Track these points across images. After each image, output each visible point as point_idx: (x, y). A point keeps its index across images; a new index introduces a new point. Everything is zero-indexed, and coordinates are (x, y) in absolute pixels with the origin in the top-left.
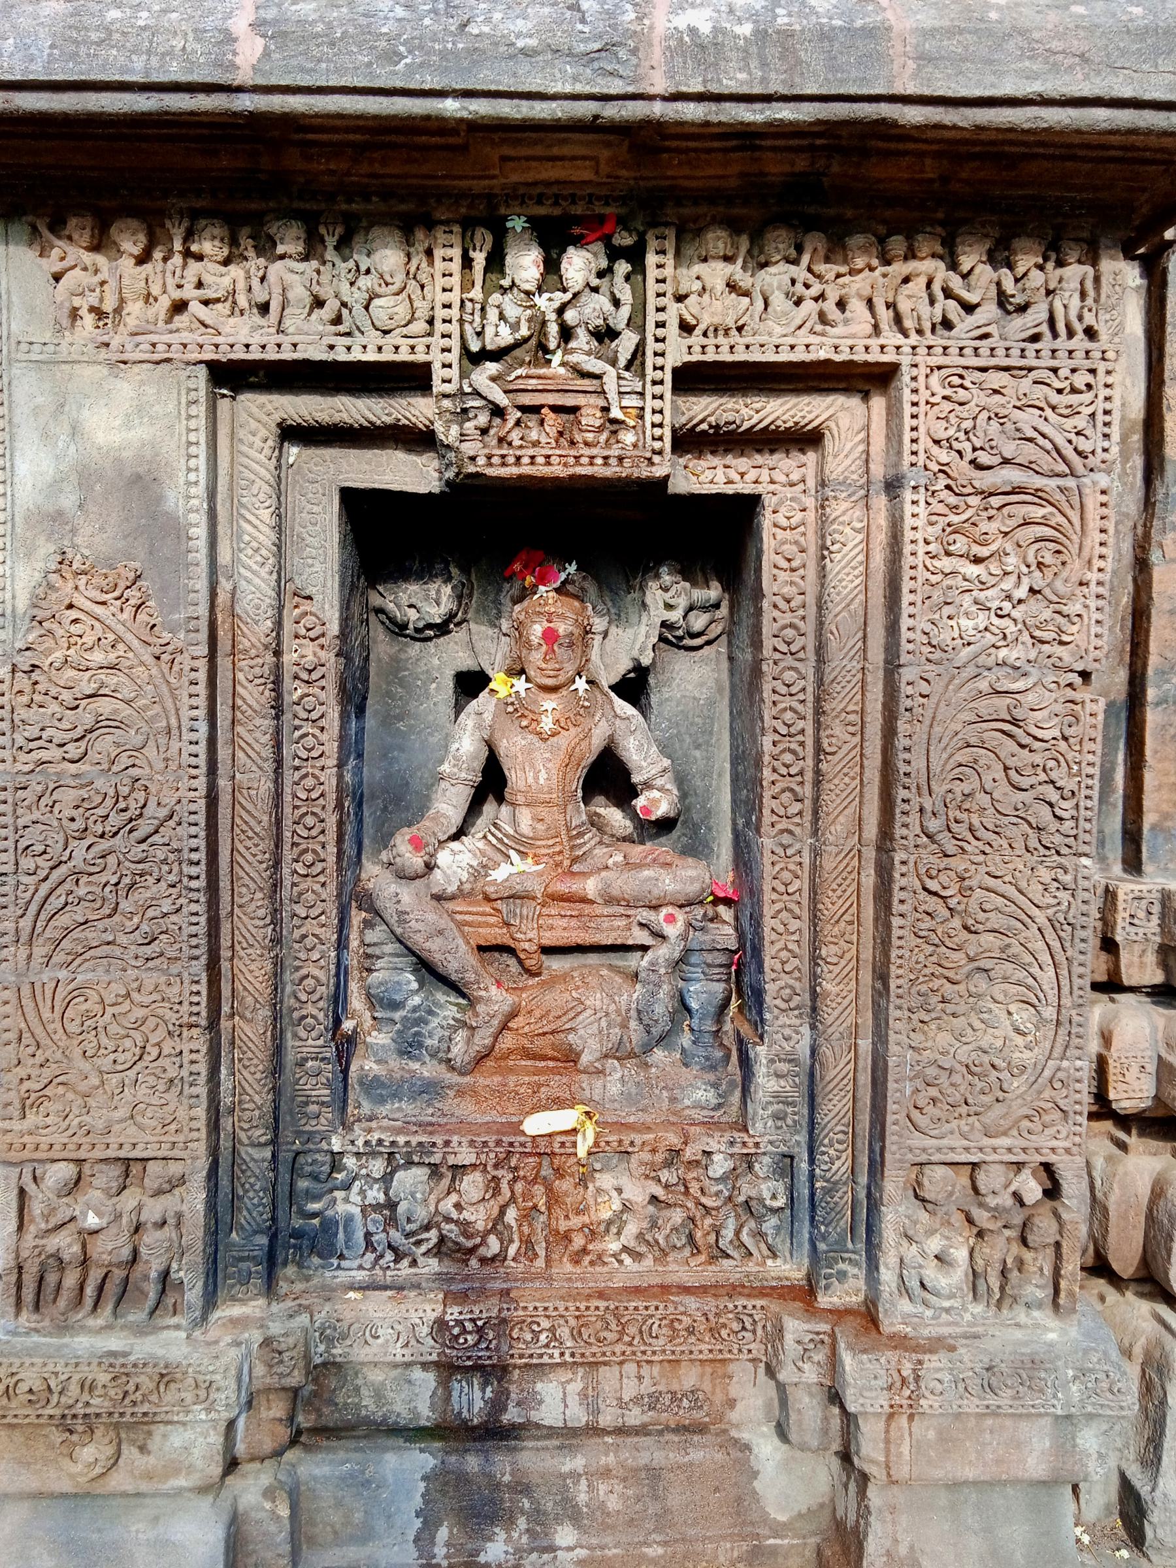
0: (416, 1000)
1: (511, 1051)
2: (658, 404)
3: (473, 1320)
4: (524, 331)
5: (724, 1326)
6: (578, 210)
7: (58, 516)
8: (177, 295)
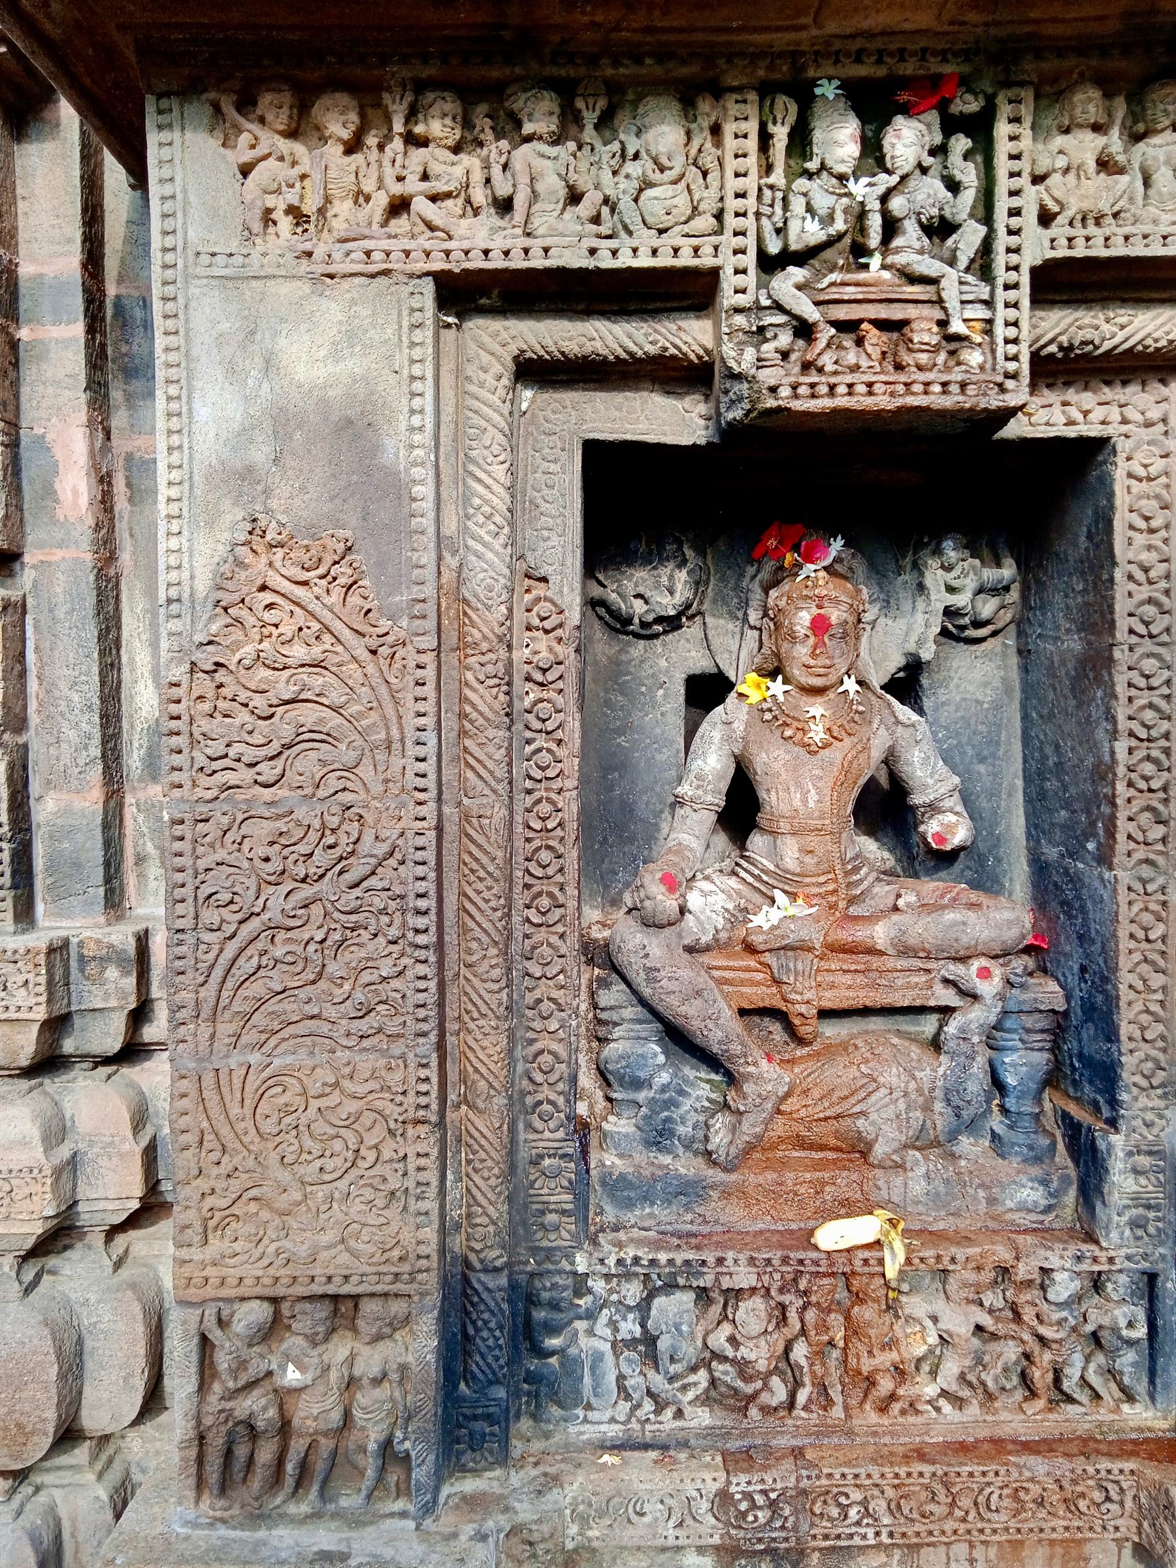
0: (664, 1077)
1: (781, 1140)
2: (1012, 314)
3: (764, 1492)
4: (840, 225)
5: (1083, 1495)
6: (909, 68)
7: (248, 474)
8: (397, 189)
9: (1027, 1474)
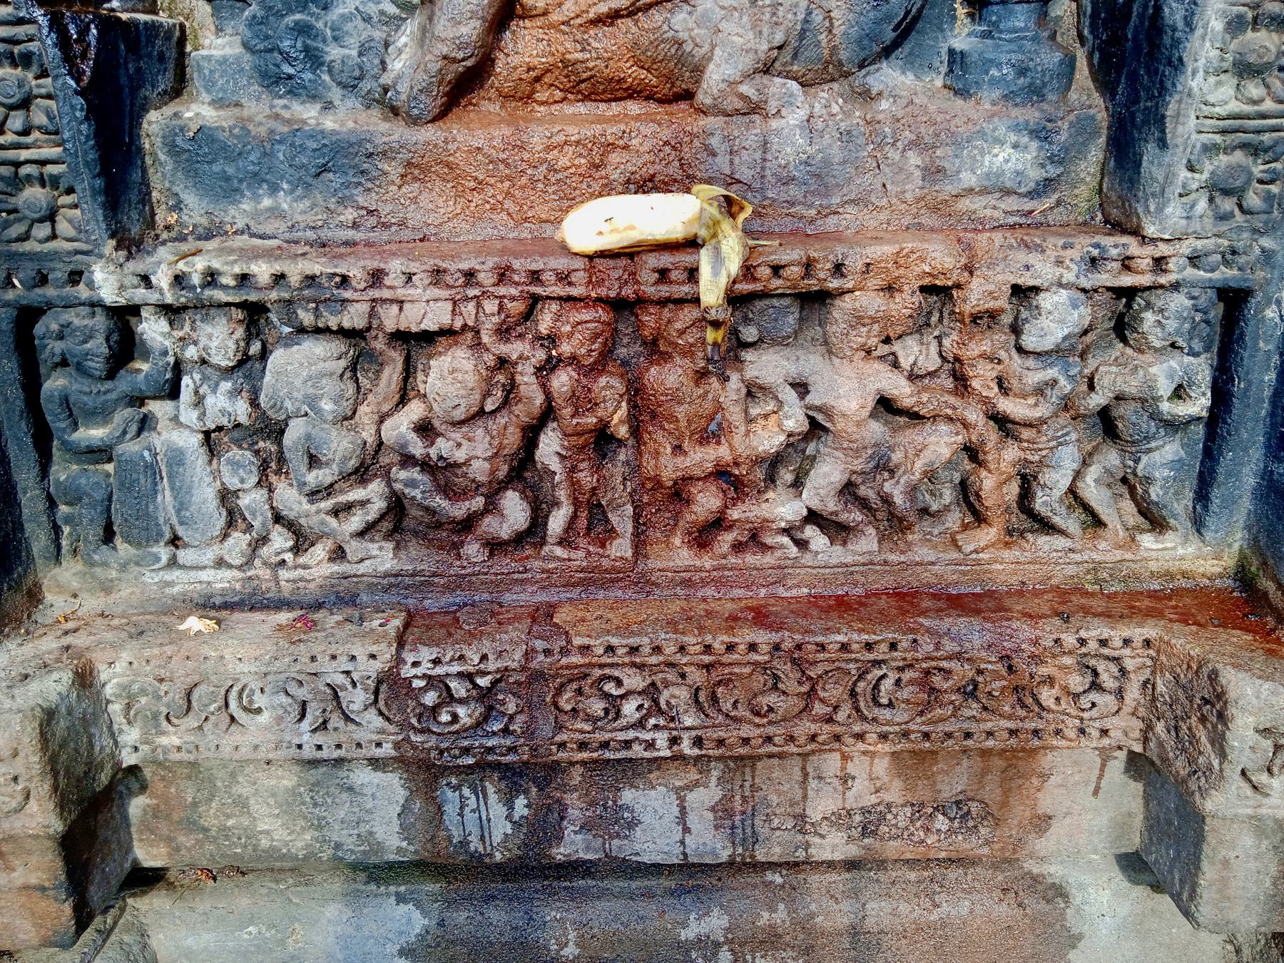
3: (469, 677)
5: (1050, 681)
9: (949, 646)
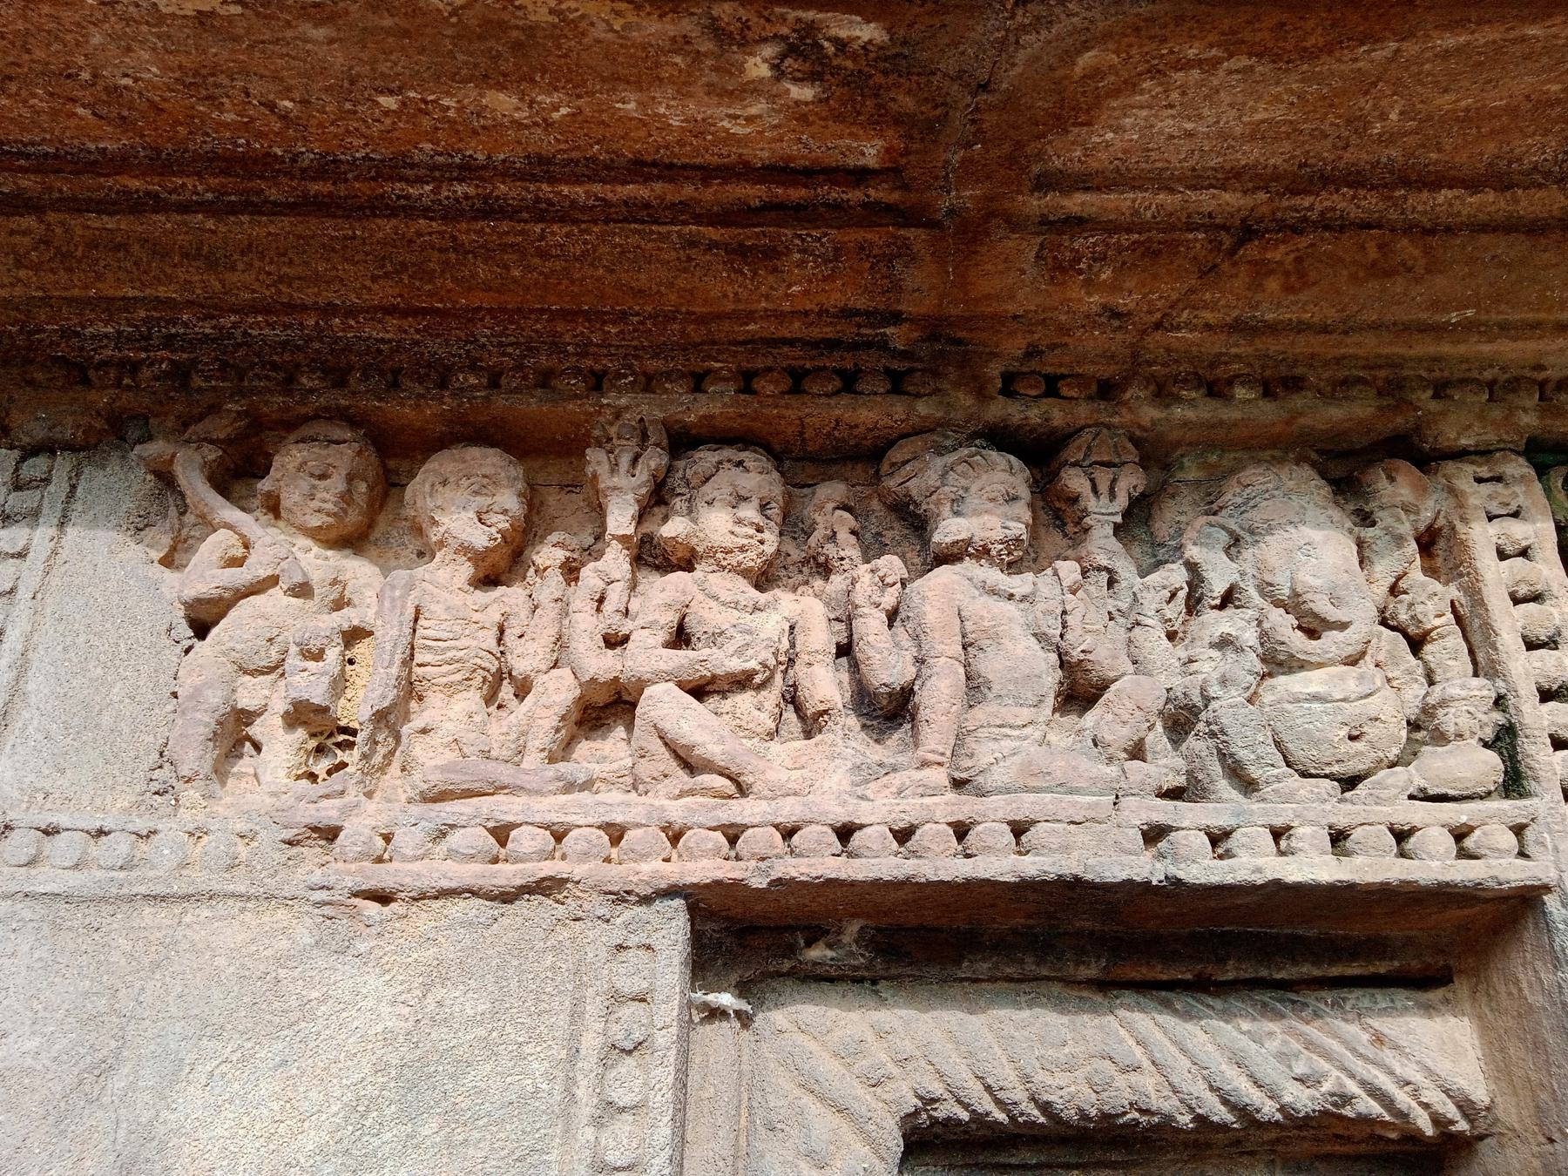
8: (604, 665)
